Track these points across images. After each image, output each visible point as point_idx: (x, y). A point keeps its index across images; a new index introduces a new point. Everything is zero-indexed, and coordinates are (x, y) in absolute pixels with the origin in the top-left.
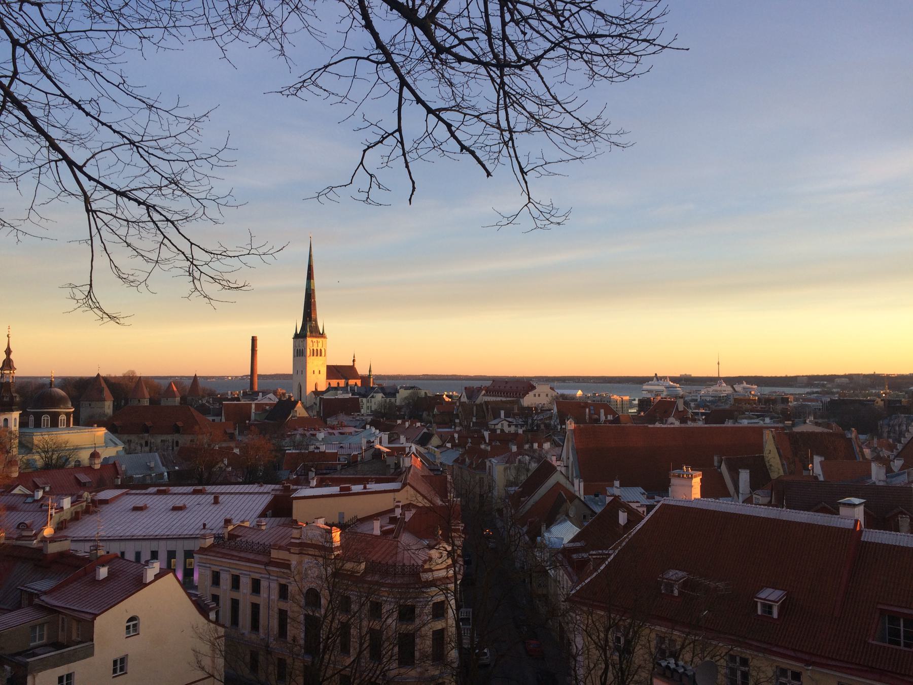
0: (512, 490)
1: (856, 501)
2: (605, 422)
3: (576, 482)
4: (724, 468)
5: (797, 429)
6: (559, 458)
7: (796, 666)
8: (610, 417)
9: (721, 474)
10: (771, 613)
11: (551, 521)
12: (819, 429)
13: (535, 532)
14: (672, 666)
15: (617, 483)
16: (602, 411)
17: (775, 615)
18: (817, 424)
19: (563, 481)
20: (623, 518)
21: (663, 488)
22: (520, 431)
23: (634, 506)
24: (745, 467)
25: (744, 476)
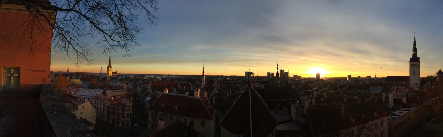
0: (141, 92)
1: (188, 92)
2: (156, 81)
5: (183, 82)
6: (148, 87)
8: (157, 81)
9: (172, 89)
10: (176, 109)
12: (185, 83)
13: (144, 99)
14: (161, 118)
15: (157, 91)
16: (155, 80)
17: (176, 109)
18: (185, 82)
19: (149, 90)
20: (157, 96)
21: (162, 91)
22: (143, 83)
23: (159, 94)
24: (175, 88)
25: (175, 89)
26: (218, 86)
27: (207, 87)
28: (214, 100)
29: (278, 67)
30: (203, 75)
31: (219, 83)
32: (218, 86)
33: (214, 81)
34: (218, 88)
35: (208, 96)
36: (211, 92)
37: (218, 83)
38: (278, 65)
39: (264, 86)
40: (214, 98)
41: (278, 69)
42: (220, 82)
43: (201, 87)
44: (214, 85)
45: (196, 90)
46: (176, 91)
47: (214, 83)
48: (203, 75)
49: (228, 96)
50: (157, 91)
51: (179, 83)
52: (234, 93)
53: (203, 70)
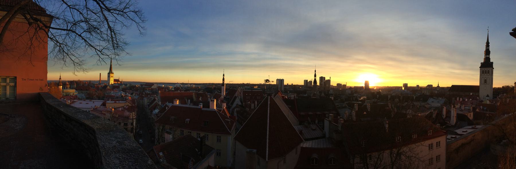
0: (148, 104)
1: (201, 104)
3: (160, 102)
4: (186, 99)
5: (198, 93)
7: (190, 131)
8: (168, 90)
10: (187, 122)
11: (154, 109)
15: (167, 102)
18: (202, 92)
22: (151, 93)
25: (189, 101)
27: (228, 97)
30: (223, 83)
31: (242, 93)
33: (237, 90)
34: (241, 98)
35: (228, 108)
36: (232, 104)
37: (240, 93)
40: (235, 109)
42: (243, 91)
43: (221, 98)
44: (236, 95)
45: (211, 101)
46: (191, 102)
47: (237, 93)
48: (223, 83)
49: (252, 107)
50: (167, 102)
51: (194, 94)
53: (223, 78)
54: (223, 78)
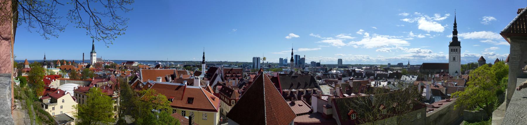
1: (185, 81)
12: (182, 70)
26: (222, 74)
28: (217, 89)
29: (292, 52)
30: (204, 60)
31: (223, 71)
32: (222, 74)
34: (221, 76)
37: (221, 71)
38: (292, 50)
39: (278, 74)
41: (292, 54)
44: (217, 72)
48: (204, 60)
52: (240, 82)
54: (203, 56)
